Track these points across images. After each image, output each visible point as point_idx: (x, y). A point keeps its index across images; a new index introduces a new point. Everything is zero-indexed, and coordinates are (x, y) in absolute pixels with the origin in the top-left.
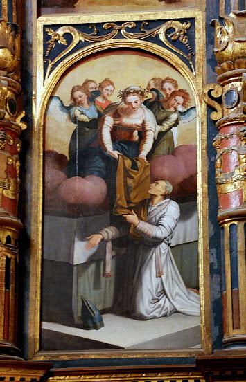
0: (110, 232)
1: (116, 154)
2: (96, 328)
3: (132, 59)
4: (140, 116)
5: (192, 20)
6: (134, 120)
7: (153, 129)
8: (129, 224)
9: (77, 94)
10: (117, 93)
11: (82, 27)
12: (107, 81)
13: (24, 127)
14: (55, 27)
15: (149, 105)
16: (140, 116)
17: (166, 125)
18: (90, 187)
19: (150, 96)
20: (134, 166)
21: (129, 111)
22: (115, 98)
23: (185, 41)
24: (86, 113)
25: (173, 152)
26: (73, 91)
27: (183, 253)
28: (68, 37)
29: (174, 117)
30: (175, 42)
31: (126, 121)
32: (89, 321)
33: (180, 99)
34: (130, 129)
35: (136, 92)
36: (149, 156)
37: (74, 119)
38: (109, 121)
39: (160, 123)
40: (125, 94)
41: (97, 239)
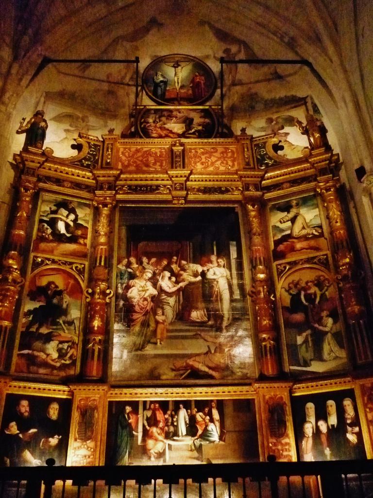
0: (309, 332)
1: (307, 304)
2: (309, 366)
3: (308, 271)
4: (313, 290)
5: (326, 255)
6: (312, 291)
7: (319, 293)
8: (316, 328)
9: (291, 285)
10: (304, 283)
11: (289, 263)
12: (300, 280)
13: (273, 299)
14: (280, 265)
15: (316, 285)
16: (313, 290)
17: (323, 291)
18: (299, 317)
19: (316, 282)
20: (314, 307)
21: (310, 288)
22: (303, 285)
23: (325, 262)
24: (294, 292)
25: (327, 300)
26: (289, 284)
27: (337, 336)
28: (285, 267)
29: (326, 288)
30: (322, 263)
31: (309, 292)
32: (306, 364)
33: (327, 282)
34: (311, 294)
35: (311, 282)
36: (319, 302)
37: (290, 294)
38: (303, 293)
39: (321, 290)
40: (307, 283)
41: (304, 334)
